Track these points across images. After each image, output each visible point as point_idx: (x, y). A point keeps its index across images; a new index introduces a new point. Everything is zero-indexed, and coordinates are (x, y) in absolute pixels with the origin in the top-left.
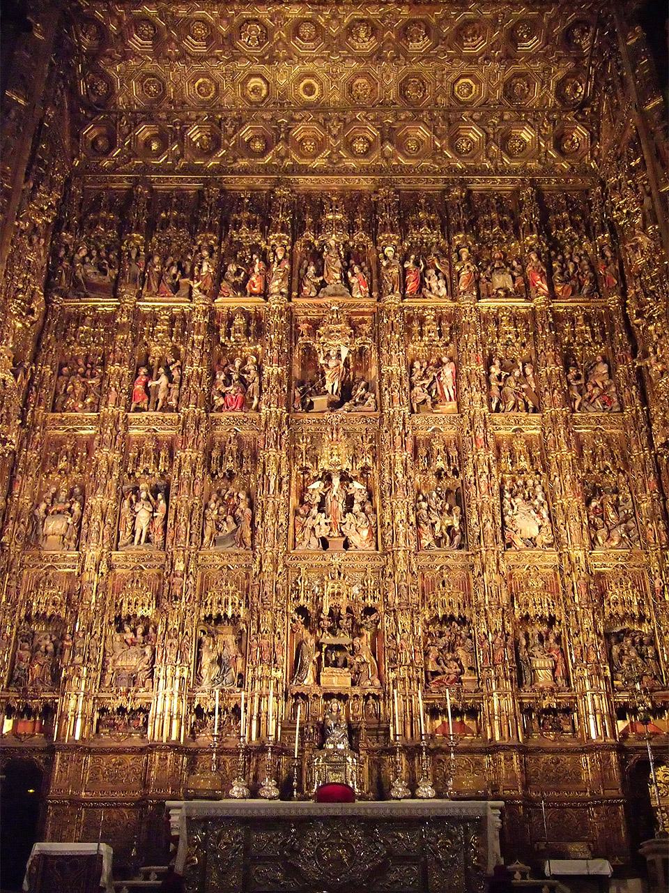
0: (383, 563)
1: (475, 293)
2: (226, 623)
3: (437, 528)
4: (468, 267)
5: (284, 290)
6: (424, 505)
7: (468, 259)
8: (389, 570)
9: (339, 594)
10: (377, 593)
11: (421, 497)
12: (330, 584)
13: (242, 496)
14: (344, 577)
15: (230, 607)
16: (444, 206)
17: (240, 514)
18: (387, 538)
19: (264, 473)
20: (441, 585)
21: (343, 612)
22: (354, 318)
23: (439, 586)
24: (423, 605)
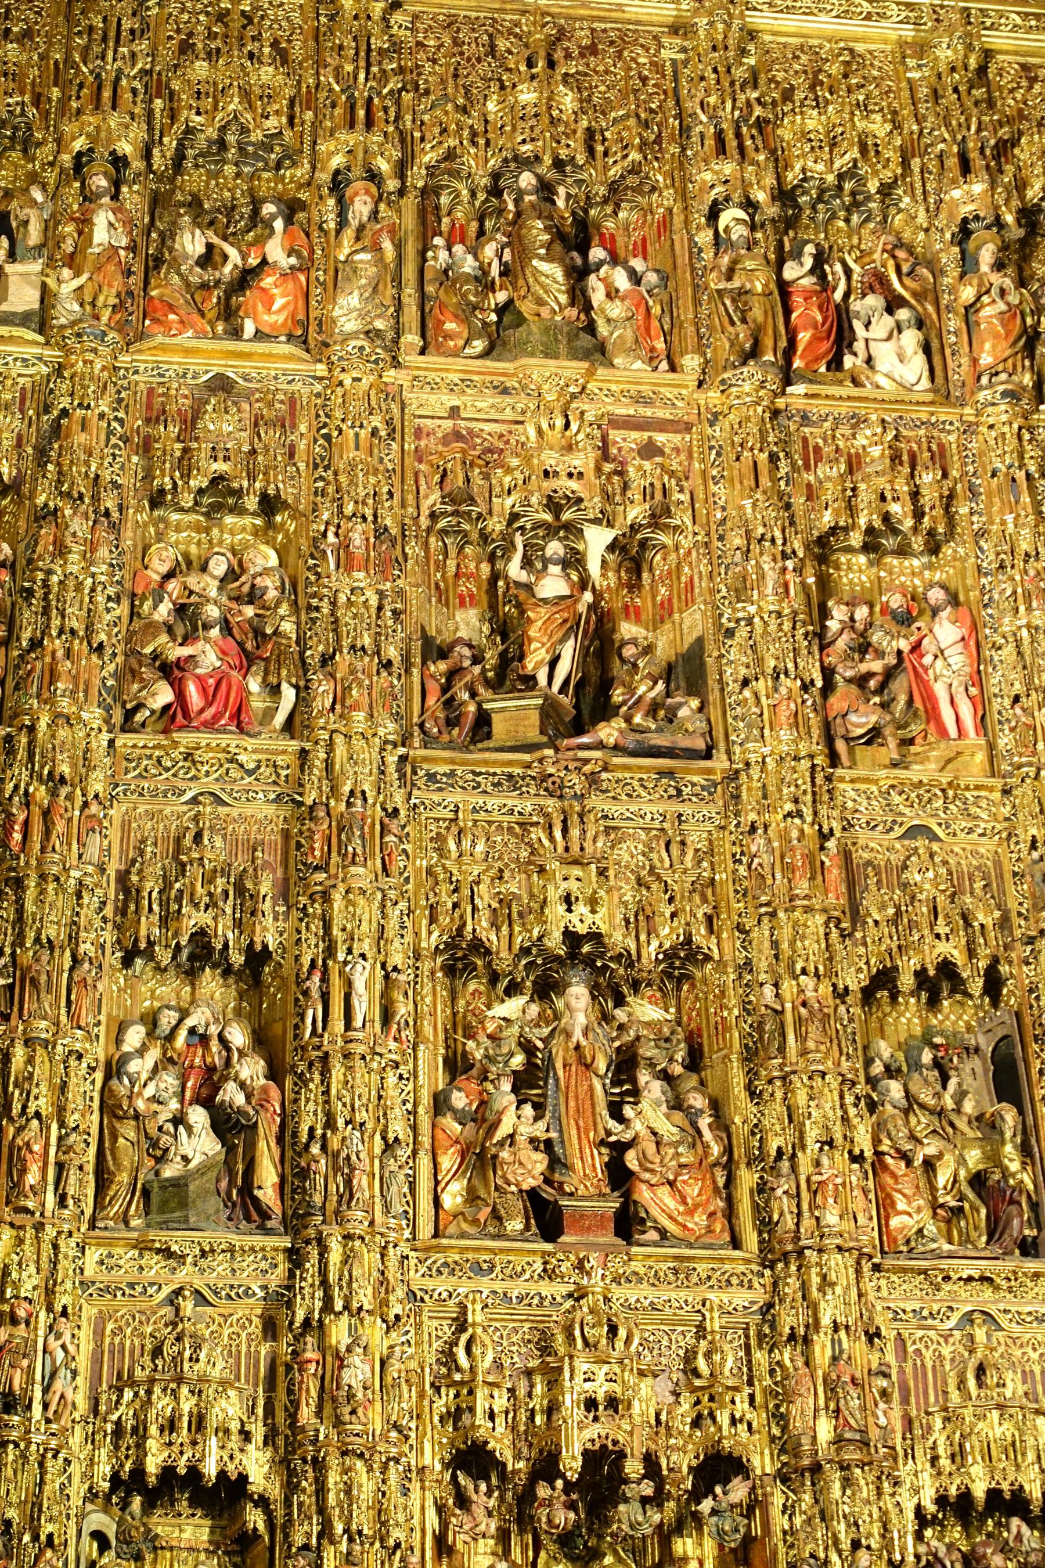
0: (759, 1296)
1: (1027, 380)
2: (183, 1507)
3: (943, 1177)
4: (1003, 293)
5: (379, 324)
6: (895, 1089)
7: (999, 266)
8: (788, 1320)
9: (612, 1403)
10: (742, 1406)
11: (877, 1068)
12: (582, 1366)
13: (238, 1037)
14: (628, 1341)
15: (213, 1442)
16: (906, 94)
17: (240, 1099)
18: (782, 1206)
19: (330, 951)
20: (972, 1383)
21: (633, 1467)
22: (615, 435)
23: (961, 1384)
24: (910, 1453)
